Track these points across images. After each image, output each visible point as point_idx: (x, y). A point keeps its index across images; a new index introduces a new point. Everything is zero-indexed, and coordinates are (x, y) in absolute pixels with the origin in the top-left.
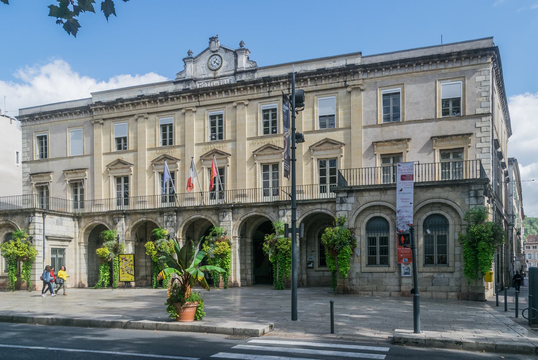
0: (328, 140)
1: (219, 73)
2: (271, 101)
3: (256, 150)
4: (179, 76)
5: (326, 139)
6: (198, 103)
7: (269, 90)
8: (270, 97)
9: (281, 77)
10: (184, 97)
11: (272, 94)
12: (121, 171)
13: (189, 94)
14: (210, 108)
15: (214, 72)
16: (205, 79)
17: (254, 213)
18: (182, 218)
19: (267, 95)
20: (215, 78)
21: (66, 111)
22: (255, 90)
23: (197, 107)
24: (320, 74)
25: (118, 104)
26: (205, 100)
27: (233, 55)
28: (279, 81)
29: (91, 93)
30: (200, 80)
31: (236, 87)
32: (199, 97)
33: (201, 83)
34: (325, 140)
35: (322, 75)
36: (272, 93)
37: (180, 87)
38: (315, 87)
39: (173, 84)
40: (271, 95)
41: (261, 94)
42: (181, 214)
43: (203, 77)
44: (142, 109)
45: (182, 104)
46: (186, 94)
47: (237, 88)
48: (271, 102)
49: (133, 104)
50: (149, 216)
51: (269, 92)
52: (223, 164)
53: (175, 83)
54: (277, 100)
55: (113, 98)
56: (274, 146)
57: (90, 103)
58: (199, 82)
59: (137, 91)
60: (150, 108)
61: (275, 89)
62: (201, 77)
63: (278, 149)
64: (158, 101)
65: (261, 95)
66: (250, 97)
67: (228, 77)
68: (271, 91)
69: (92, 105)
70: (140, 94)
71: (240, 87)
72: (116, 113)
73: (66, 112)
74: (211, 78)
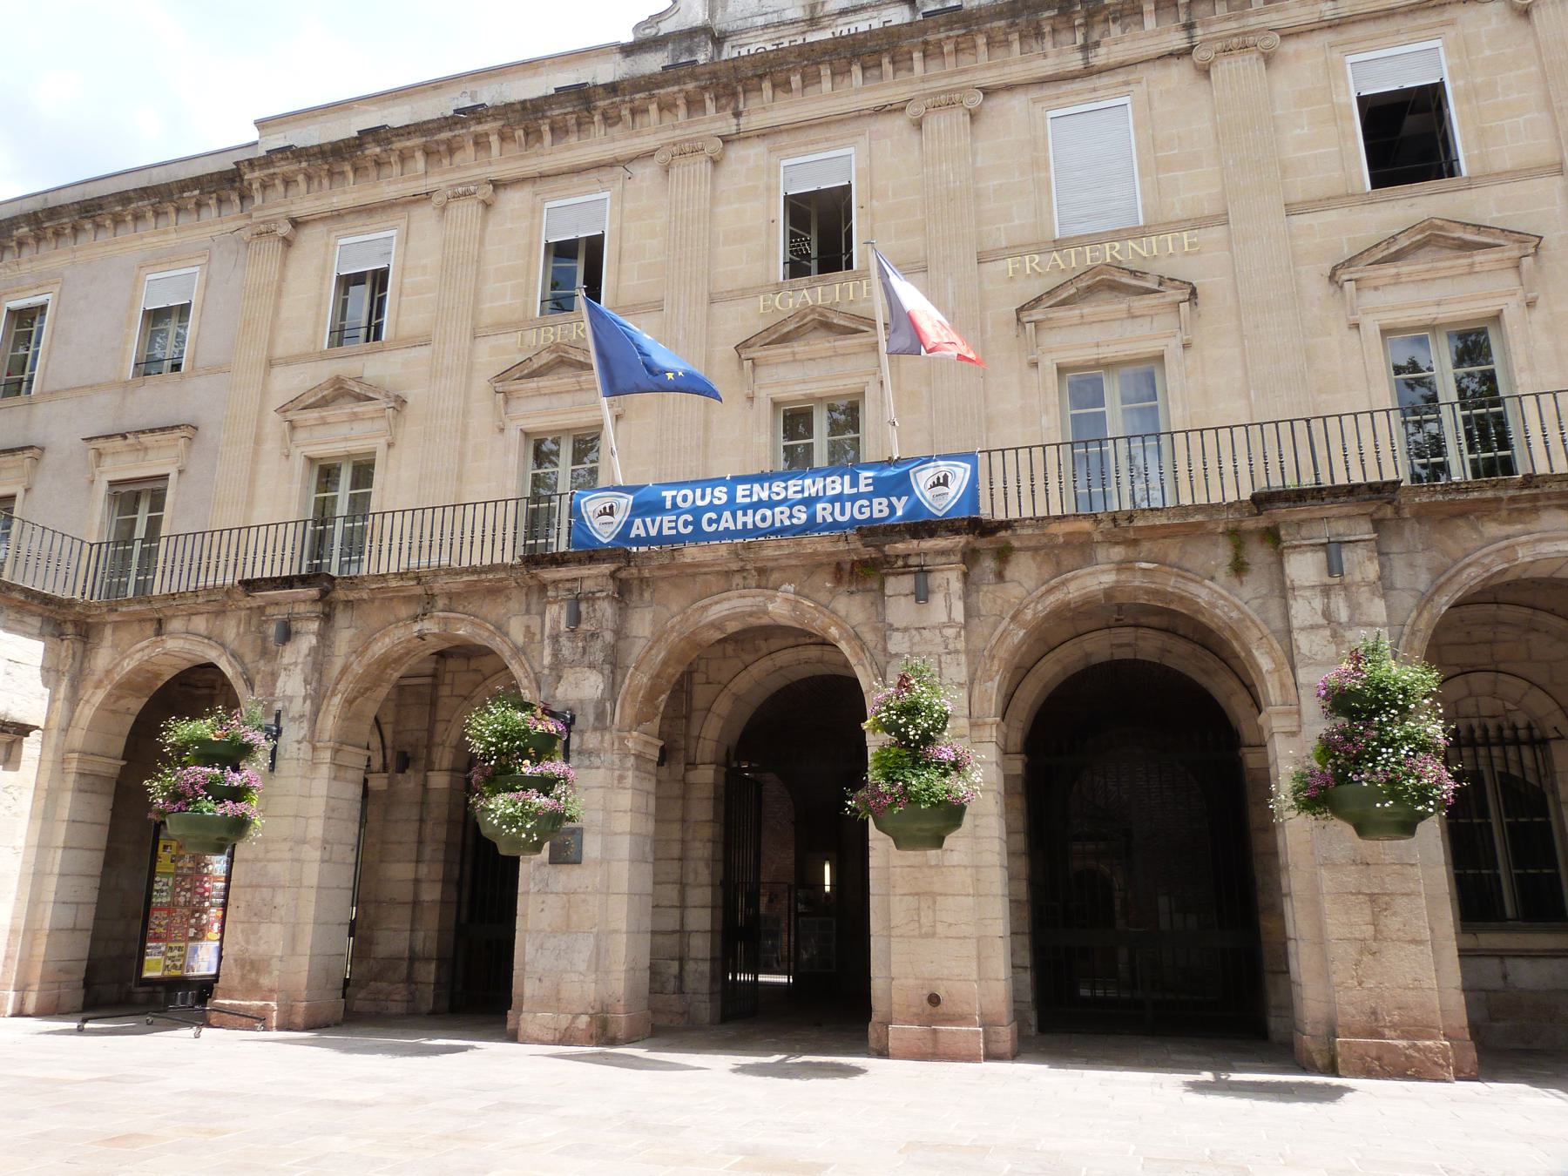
0: (1441, 228)
2: (1095, 90)
4: (647, 31)
5: (1429, 224)
6: (734, 121)
7: (1086, 39)
8: (1089, 72)
10: (666, 107)
12: (343, 430)
13: (690, 86)
14: (784, 140)
16: (766, 27)
17: (1109, 579)
18: (648, 616)
19: (1075, 61)
21: (141, 199)
22: (1016, 46)
25: (367, 152)
26: (765, 110)
29: (261, 124)
32: (734, 94)
33: (747, 48)
34: (1423, 231)
36: (1102, 51)
37: (653, 63)
39: (618, 57)
41: (1044, 62)
42: (647, 595)
43: (760, 21)
44: (470, 167)
45: (653, 132)
46: (676, 88)
47: (926, 43)
48: (1101, 93)
49: (428, 153)
50: (461, 608)
52: (857, 380)
53: (628, 50)
54: (1127, 83)
55: (347, 128)
56: (1133, 273)
57: (248, 154)
58: (740, 42)
60: (503, 162)
61: (1115, 29)
63: (1155, 287)
64: (546, 128)
65: (1046, 67)
67: (875, 14)
68: (1097, 44)
69: (251, 163)
71: (942, 35)
72: (349, 194)
73: (140, 204)
74: (793, 22)
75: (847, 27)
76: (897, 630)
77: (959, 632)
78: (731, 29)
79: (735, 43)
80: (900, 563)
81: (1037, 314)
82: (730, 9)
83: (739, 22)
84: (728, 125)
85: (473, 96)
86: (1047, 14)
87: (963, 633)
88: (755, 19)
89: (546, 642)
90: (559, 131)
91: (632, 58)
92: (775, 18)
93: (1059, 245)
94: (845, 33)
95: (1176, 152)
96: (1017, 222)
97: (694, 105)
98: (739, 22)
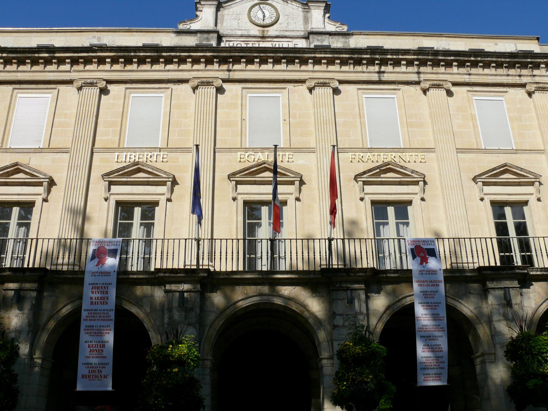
1: (272, 31)
3: (364, 173)
4: (185, 26)
8: (380, 82)
9: (406, 52)
11: (386, 77)
13: (208, 54)
15: (262, 29)
16: (242, 36)
19: (375, 77)
20: (263, 37)
23: (224, 81)
24: (470, 57)
27: (301, 9)
28: (401, 57)
30: (231, 36)
31: (313, 55)
35: (479, 59)
36: (385, 75)
38: (468, 76)
40: (383, 79)
43: (239, 33)
51: (379, 72)
59: (91, 37)
62: (233, 33)
63: (410, 174)
66: (342, 77)
70: (95, 42)
71: (322, 56)
75: (278, 43)
76: (338, 315)
77: (364, 317)
78: (225, 33)
79: (227, 39)
80: (338, 285)
81: (365, 178)
82: (224, 24)
83: (229, 31)
84: (225, 75)
85: (99, 38)
86: (365, 56)
87: (366, 317)
88: (237, 31)
89: (166, 311)
90: (142, 61)
91: (180, 37)
92: (245, 33)
93: (371, 150)
94: (277, 46)
95: (414, 120)
96: (352, 138)
97: (209, 61)
98: (229, 31)
